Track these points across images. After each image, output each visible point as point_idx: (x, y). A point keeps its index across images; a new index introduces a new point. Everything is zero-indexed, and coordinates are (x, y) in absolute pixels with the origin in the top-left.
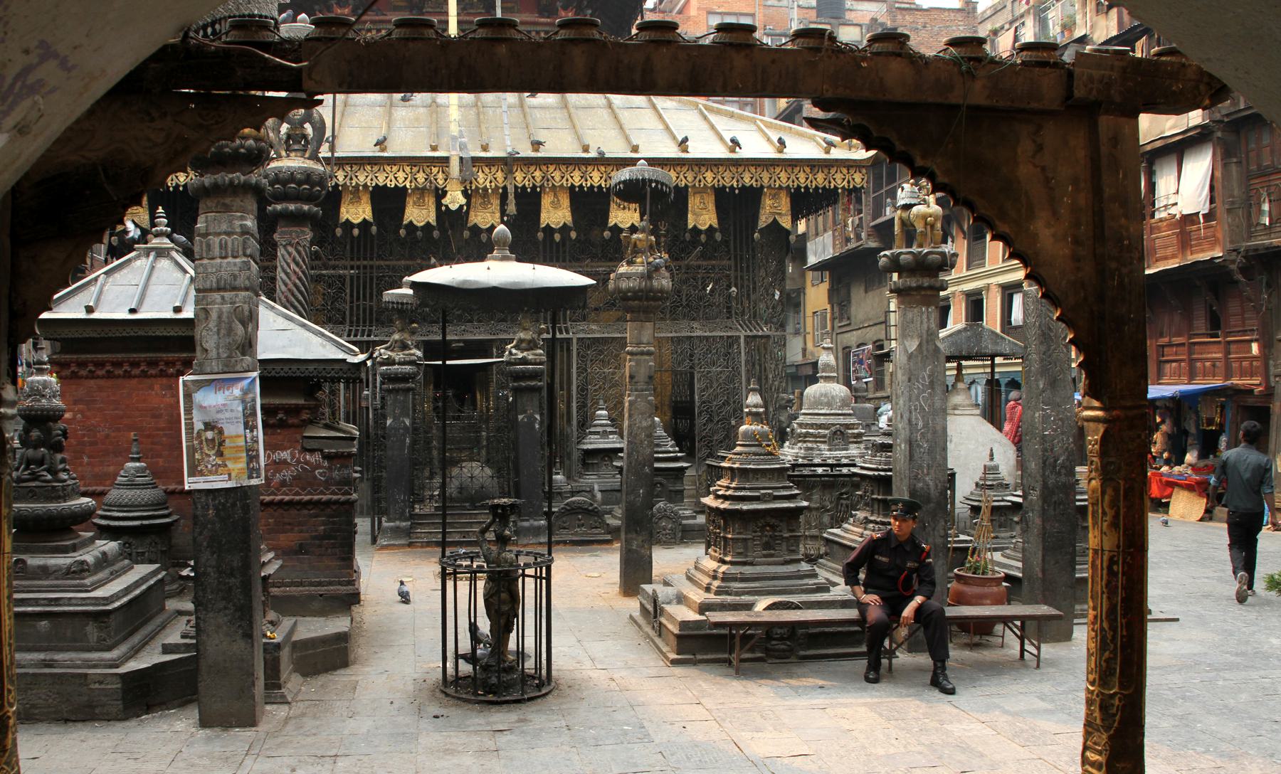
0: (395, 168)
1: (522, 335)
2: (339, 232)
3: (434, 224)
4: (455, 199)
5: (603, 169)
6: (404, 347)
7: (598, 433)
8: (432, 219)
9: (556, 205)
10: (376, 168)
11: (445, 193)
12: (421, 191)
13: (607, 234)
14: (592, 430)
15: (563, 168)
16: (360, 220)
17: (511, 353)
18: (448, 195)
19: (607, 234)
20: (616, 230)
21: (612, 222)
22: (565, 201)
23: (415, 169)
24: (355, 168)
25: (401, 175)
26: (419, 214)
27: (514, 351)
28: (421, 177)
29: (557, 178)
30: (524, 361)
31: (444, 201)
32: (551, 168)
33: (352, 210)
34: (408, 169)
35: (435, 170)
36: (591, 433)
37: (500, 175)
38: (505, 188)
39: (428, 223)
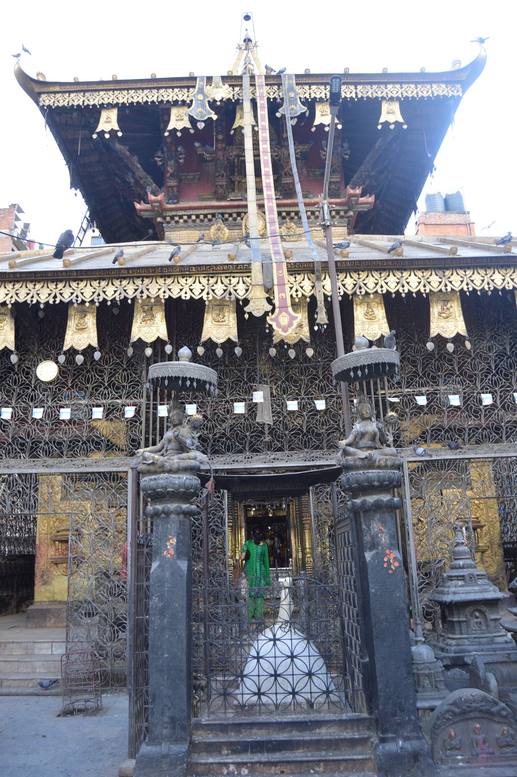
0: (190, 281)
1: (358, 427)
2: (130, 351)
3: (235, 339)
4: (257, 307)
5: (419, 274)
6: (182, 448)
7: (462, 578)
8: (233, 334)
9: (370, 317)
10: (169, 281)
11: (246, 302)
12: (220, 305)
13: (430, 346)
14: (455, 573)
15: (376, 274)
16: (154, 339)
17: (346, 453)
18: (251, 303)
19: (430, 346)
20: (440, 340)
21: (434, 331)
22: (380, 312)
23: (212, 281)
24: (146, 281)
25: (197, 288)
26: (219, 328)
27: (351, 449)
28: (219, 289)
29: (371, 285)
30: (369, 464)
31: (246, 309)
32: (363, 275)
33: (144, 329)
34: (204, 281)
35: (234, 281)
36: (450, 578)
37: (307, 284)
38: (313, 298)
39: (229, 339)
